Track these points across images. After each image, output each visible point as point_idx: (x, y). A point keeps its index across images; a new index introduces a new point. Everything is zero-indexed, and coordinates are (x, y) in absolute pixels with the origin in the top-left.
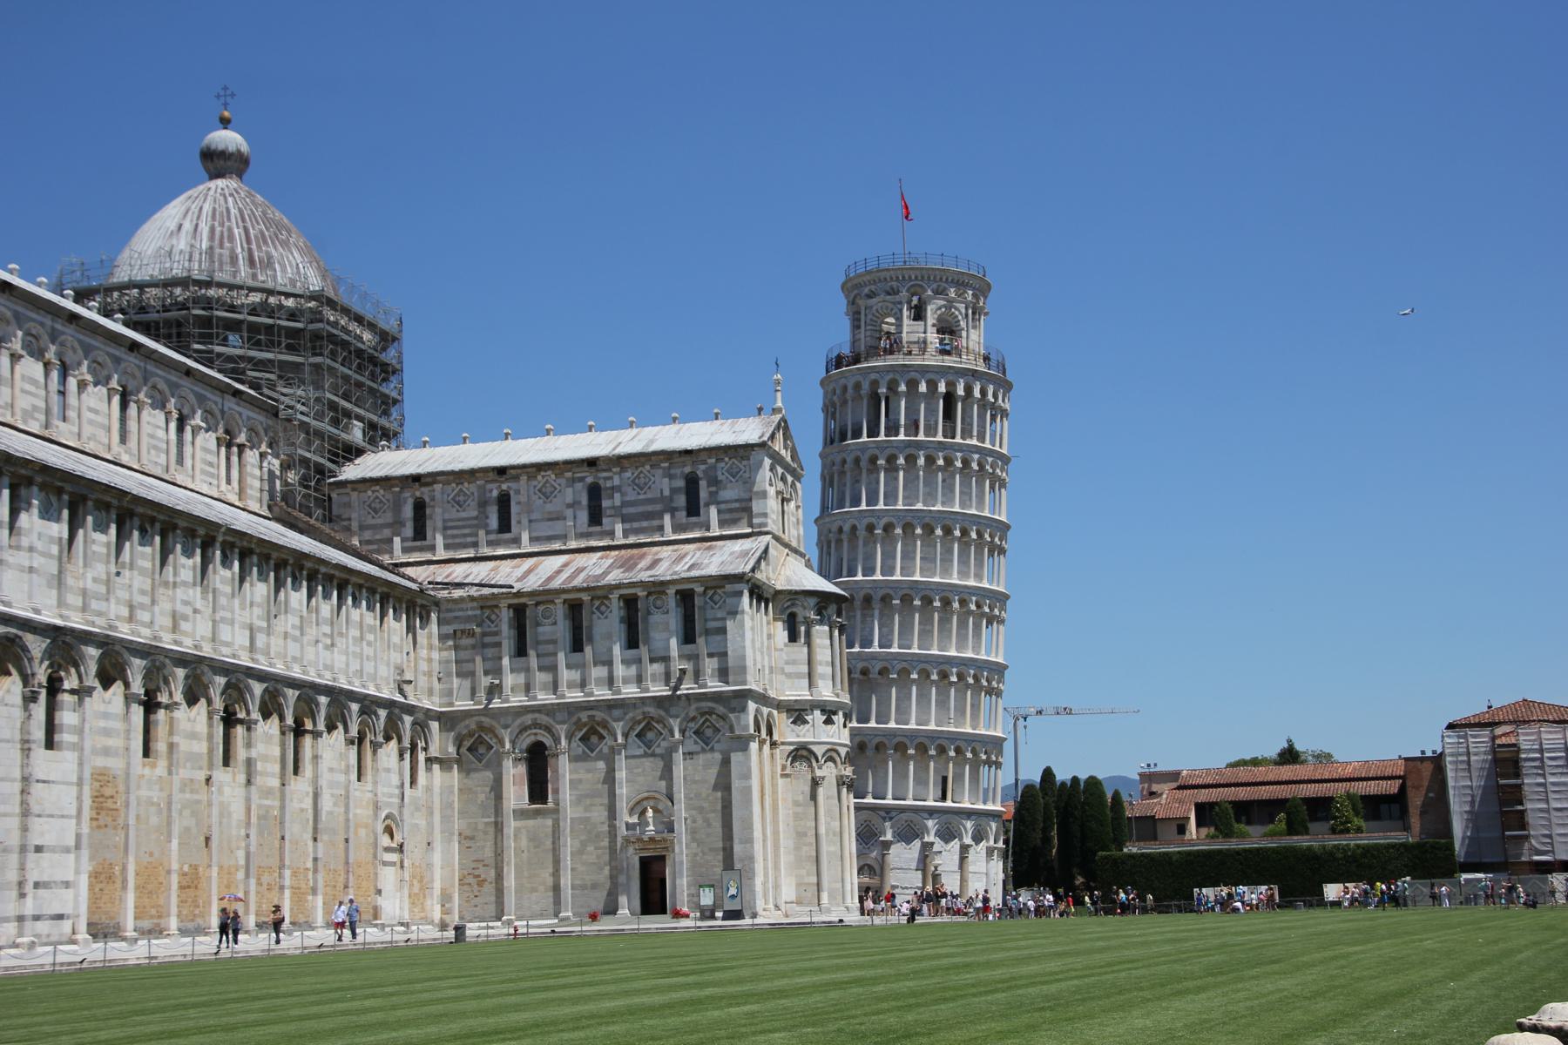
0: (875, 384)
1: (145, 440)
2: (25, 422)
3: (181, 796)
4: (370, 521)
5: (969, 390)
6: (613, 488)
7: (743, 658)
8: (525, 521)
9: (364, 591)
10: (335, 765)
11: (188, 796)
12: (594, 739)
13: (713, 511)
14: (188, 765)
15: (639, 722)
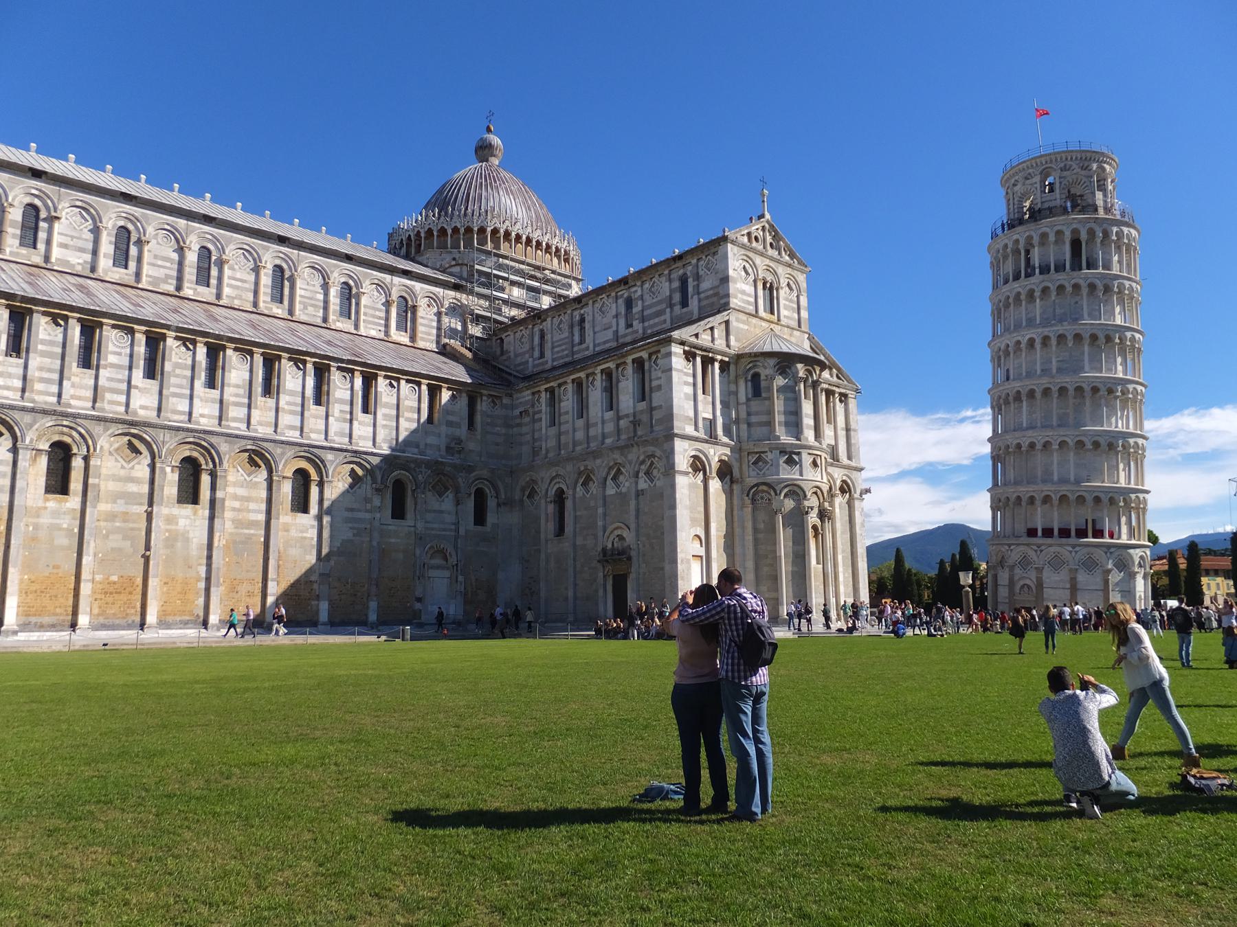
0: (1017, 241)
1: (298, 299)
2: (150, 283)
3: (102, 524)
4: (520, 351)
5: (1091, 233)
6: (637, 299)
7: (671, 407)
8: (591, 334)
9: (403, 382)
10: (355, 506)
11: (118, 524)
12: (591, 483)
13: (696, 297)
14: (118, 501)
15: (611, 468)
